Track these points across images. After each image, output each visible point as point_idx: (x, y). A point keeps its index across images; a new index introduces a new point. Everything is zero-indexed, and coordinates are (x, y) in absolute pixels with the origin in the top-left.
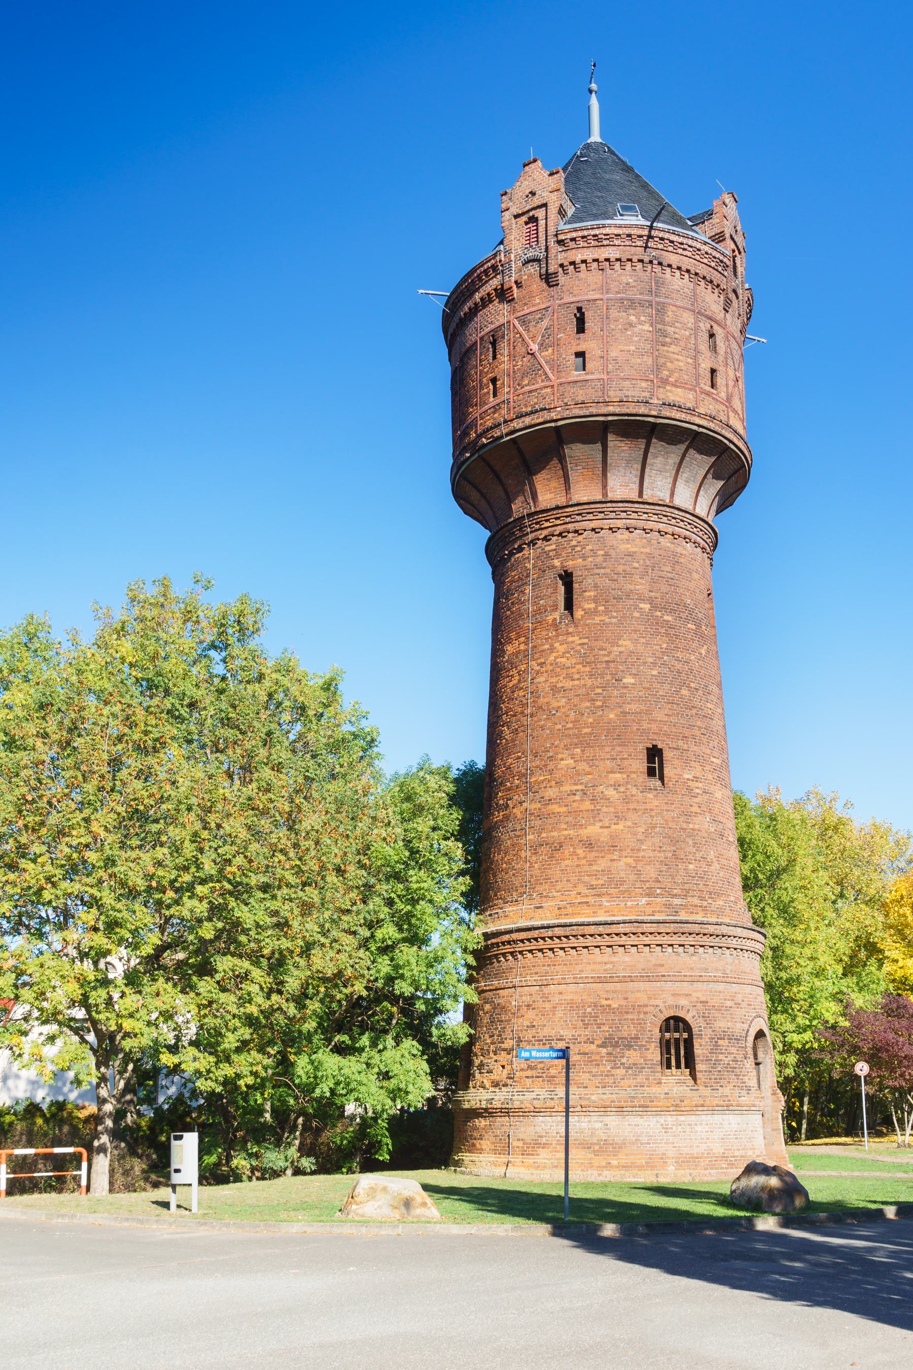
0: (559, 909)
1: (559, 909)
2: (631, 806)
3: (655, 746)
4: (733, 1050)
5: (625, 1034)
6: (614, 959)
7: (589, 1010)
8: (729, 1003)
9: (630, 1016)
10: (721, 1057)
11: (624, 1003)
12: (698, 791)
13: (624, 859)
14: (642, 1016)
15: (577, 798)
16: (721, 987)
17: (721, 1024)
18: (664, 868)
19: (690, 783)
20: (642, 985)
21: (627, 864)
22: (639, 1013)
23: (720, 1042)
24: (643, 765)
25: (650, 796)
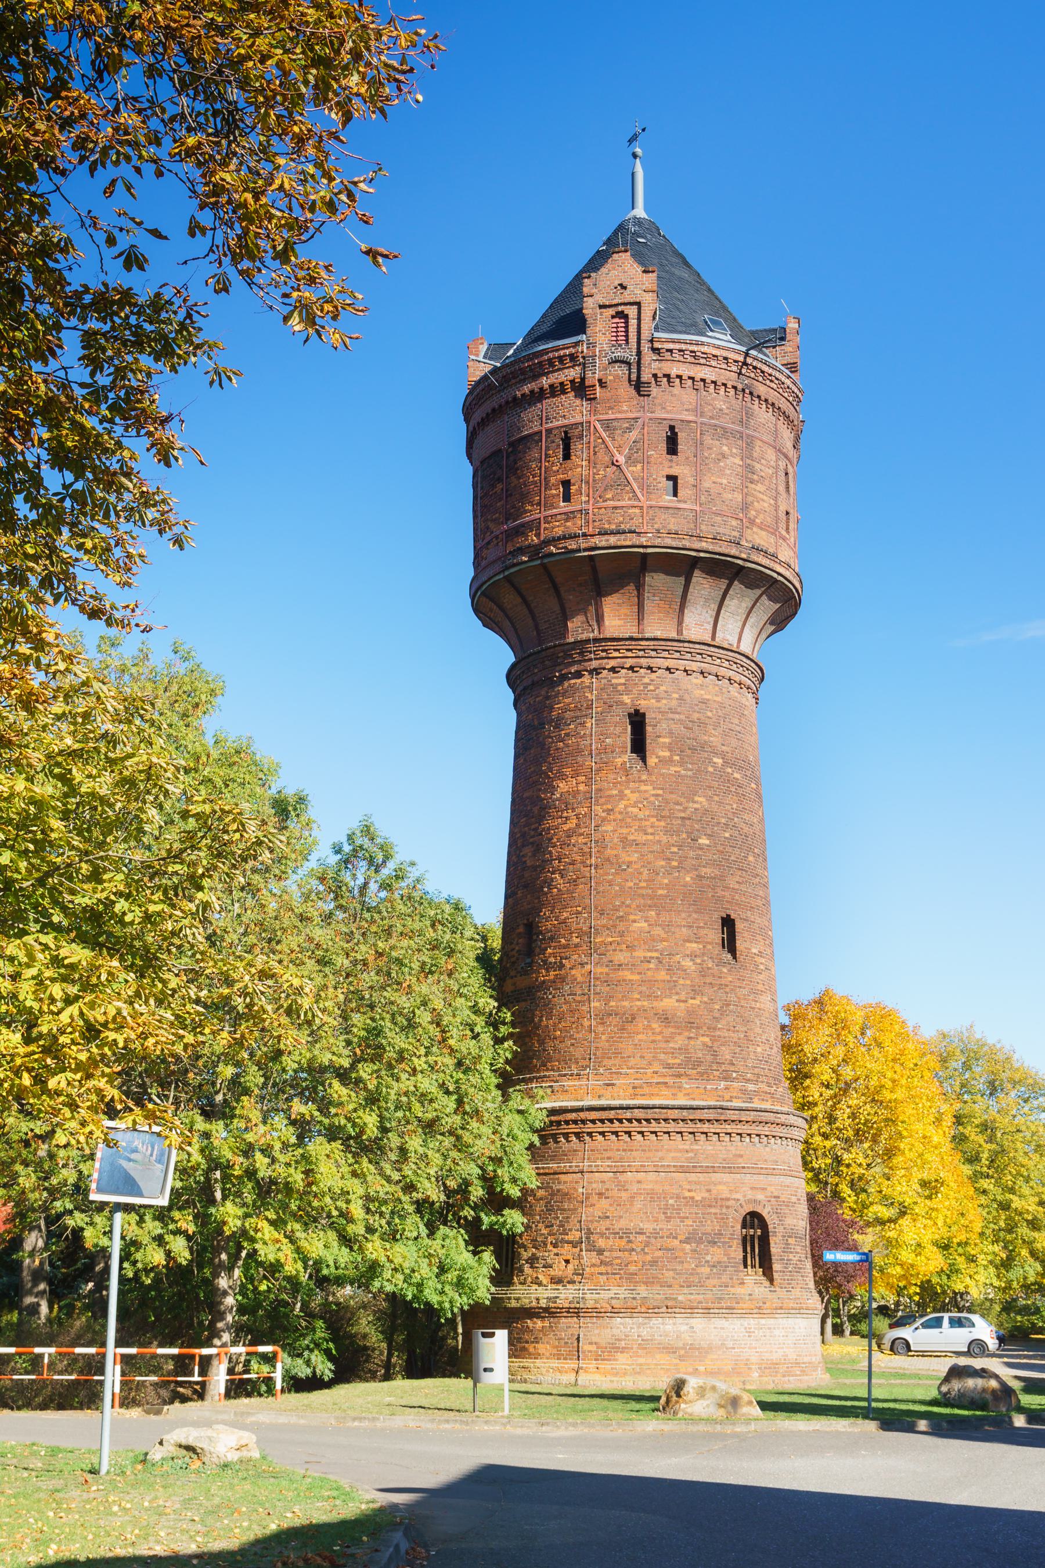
2: (708, 980)
3: (728, 916)
5: (709, 1229)
7: (671, 1202)
9: (713, 1210)
11: (706, 1195)
13: (701, 1039)
14: (724, 1210)
15: (652, 966)
20: (726, 1177)
21: (704, 1044)
25: (725, 970)
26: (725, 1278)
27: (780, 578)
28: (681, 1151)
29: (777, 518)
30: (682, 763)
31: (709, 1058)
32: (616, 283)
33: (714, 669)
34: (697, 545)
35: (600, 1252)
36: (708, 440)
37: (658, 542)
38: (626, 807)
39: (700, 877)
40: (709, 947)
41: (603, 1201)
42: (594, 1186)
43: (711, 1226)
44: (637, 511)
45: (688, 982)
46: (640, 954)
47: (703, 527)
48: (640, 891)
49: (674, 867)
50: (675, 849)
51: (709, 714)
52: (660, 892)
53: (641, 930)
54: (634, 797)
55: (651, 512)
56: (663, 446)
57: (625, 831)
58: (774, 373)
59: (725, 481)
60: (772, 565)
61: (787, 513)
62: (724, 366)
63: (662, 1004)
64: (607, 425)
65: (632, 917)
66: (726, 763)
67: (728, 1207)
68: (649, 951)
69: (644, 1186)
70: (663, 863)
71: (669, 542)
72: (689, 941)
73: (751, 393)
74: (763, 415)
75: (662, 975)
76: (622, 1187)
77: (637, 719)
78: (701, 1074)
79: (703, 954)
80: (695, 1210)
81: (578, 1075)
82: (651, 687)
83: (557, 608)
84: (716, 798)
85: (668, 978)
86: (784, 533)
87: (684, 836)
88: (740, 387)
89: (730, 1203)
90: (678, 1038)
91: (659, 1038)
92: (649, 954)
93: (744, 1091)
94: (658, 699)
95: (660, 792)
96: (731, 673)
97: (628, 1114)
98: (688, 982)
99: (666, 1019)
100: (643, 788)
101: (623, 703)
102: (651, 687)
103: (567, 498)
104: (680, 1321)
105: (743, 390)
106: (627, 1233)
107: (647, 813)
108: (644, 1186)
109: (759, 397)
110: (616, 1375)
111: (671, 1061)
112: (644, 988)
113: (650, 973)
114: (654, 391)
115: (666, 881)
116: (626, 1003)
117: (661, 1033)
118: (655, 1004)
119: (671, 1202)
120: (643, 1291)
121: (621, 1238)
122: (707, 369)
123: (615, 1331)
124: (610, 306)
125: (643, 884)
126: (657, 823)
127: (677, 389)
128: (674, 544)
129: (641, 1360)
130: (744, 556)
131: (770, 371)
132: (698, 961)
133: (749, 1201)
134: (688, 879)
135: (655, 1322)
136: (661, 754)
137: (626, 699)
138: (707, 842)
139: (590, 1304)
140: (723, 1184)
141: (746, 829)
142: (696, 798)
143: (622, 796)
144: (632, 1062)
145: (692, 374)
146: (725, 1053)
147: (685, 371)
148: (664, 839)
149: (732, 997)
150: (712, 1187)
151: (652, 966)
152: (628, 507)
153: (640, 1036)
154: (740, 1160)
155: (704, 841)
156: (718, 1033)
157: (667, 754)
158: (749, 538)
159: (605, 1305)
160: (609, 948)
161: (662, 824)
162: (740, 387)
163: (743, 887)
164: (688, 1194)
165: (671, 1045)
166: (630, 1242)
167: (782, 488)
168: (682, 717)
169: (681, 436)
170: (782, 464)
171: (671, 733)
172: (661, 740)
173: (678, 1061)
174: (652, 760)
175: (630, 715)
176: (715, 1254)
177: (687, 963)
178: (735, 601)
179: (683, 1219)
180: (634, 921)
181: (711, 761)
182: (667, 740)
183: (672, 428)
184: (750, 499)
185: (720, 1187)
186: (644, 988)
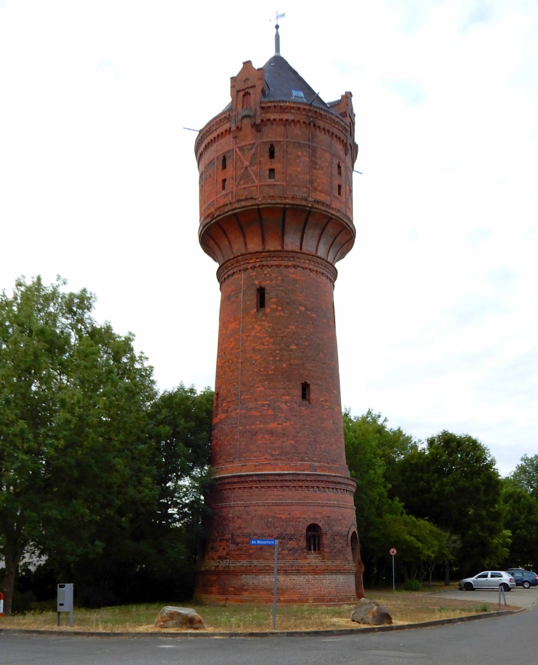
0: (255, 466)
1: (255, 466)
2: (294, 413)
3: (306, 383)
4: (342, 541)
5: (288, 532)
6: (284, 493)
7: (270, 520)
8: (340, 518)
9: (291, 523)
10: (336, 545)
11: (288, 516)
12: (327, 407)
13: (289, 441)
14: (297, 523)
15: (265, 408)
16: (336, 509)
17: (336, 528)
18: (309, 447)
19: (323, 403)
20: (298, 508)
21: (291, 444)
22: (296, 521)
23: (336, 537)
24: (299, 392)
25: (303, 408)
26: (296, 556)
30: (282, 310)
34: (284, 201)
35: (237, 544)
37: (264, 202)
39: (291, 364)
40: (295, 397)
43: (290, 530)
45: (283, 415)
46: (260, 403)
49: (278, 360)
50: (278, 352)
52: (270, 372)
57: (255, 345)
63: (270, 426)
65: (257, 385)
67: (299, 522)
68: (265, 401)
70: (272, 359)
71: (269, 201)
72: (284, 395)
75: (270, 412)
76: (248, 513)
78: (289, 459)
79: (292, 401)
84: (301, 326)
85: (273, 413)
87: (283, 345)
89: (299, 520)
91: (268, 442)
92: (265, 403)
95: (271, 325)
97: (250, 479)
98: (283, 415)
99: (271, 433)
106: (249, 535)
107: (265, 335)
110: (242, 602)
111: (274, 453)
113: (264, 411)
115: (273, 367)
116: (253, 427)
117: (269, 440)
118: (267, 426)
120: (255, 562)
121: (246, 537)
123: (243, 582)
126: (269, 340)
128: (272, 202)
129: (254, 595)
132: (289, 404)
133: (312, 519)
134: (284, 366)
135: (261, 577)
138: (295, 347)
139: (232, 569)
143: (253, 328)
148: (273, 347)
151: (265, 408)
153: (260, 442)
155: (293, 347)
157: (275, 306)
159: (238, 569)
161: (272, 340)
165: (274, 445)
171: (277, 296)
172: (273, 300)
173: (277, 453)
176: (292, 544)
177: (283, 406)
179: (275, 528)
182: (275, 300)
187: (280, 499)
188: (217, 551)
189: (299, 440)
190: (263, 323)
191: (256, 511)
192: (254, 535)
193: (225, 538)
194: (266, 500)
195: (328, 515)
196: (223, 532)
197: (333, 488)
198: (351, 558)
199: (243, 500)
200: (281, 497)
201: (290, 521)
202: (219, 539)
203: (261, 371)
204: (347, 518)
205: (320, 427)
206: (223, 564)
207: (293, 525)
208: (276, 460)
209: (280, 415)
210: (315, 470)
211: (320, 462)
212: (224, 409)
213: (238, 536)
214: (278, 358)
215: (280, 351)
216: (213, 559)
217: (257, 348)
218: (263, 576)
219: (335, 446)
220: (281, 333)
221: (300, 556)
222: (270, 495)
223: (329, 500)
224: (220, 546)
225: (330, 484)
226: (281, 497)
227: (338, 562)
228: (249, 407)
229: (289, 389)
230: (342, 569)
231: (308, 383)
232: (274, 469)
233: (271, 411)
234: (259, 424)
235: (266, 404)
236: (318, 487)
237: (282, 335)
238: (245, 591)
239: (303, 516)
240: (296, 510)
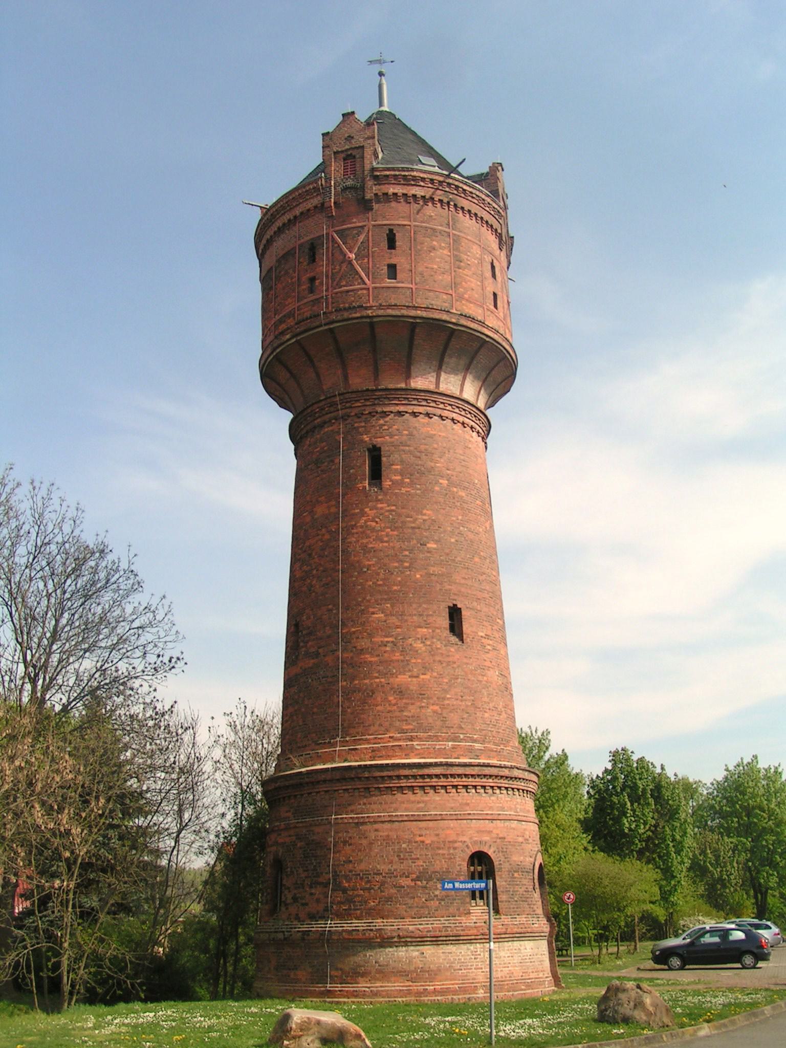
0: (373, 751)
1: (373, 751)
2: (437, 658)
3: (455, 605)
4: (525, 882)
5: (438, 868)
6: (426, 798)
7: (404, 846)
8: (520, 839)
9: (441, 852)
10: (517, 888)
11: (435, 839)
12: (489, 647)
13: (431, 707)
14: (452, 851)
15: (388, 649)
16: (514, 824)
17: (515, 858)
18: (466, 716)
19: (483, 640)
20: (452, 824)
21: (434, 712)
22: (449, 848)
23: (516, 875)
24: (445, 622)
25: (452, 650)
27: (487, 339)
28: (413, 802)
29: (484, 296)
31: (439, 723)
32: (346, 135)
33: (439, 412)
36: (420, 238)
38: (366, 521)
41: (347, 848)
42: (340, 835)
44: (365, 292)
45: (419, 661)
47: (419, 300)
48: (378, 588)
49: (406, 568)
50: (407, 553)
51: (435, 446)
53: (379, 620)
54: (372, 513)
55: (376, 291)
56: (385, 244)
58: (474, 191)
59: (435, 267)
60: (480, 328)
61: (495, 295)
62: (430, 185)
64: (341, 233)
66: (451, 484)
67: (455, 848)
69: (381, 834)
73: (455, 205)
74: (466, 222)
77: (375, 453)
80: (425, 852)
81: (329, 742)
82: (386, 427)
83: (313, 375)
85: (402, 658)
86: (492, 307)
88: (445, 200)
89: (456, 845)
90: (410, 707)
92: (386, 639)
93: (471, 750)
94: (391, 436)
95: (393, 508)
96: (466, 420)
98: (419, 661)
100: (380, 506)
101: (362, 441)
102: (386, 427)
103: (311, 291)
104: (412, 948)
105: (448, 203)
107: (383, 525)
108: (381, 834)
109: (462, 208)
112: (381, 668)
113: (386, 655)
114: (376, 206)
119: (404, 846)
122: (417, 188)
124: (342, 152)
125: (381, 583)
126: (391, 533)
127: (393, 204)
130: (454, 320)
131: (471, 190)
133: (475, 842)
134: (418, 576)
136: (394, 478)
137: (366, 438)
138: (435, 546)
140: (450, 829)
141: (471, 536)
142: (425, 511)
143: (363, 513)
144: (372, 729)
145: (405, 192)
146: (454, 718)
147: (399, 190)
149: (459, 672)
150: (440, 832)
151: (388, 649)
152: (358, 290)
153: (379, 708)
154: (468, 808)
156: (447, 702)
157: (399, 478)
158: (459, 308)
160: (354, 636)
161: (395, 533)
162: (445, 200)
163: (469, 583)
164: (418, 839)
165: (405, 714)
166: (369, 882)
167: (488, 274)
168: (412, 448)
169: (398, 236)
170: (488, 259)
171: (402, 462)
173: (412, 727)
174: (386, 483)
175: (369, 450)
177: (418, 645)
178: (454, 360)
180: (373, 613)
181: (437, 482)
183: (391, 231)
184: (458, 280)
185: (448, 832)
186: (381, 668)
187: (418, 810)
188: (306, 904)
189: (448, 704)
190: (380, 506)
191: (376, 830)
192: (374, 874)
193: (321, 880)
194: (396, 810)
195: (501, 835)
196: (315, 869)
197: (507, 788)
198: (540, 911)
199: (352, 811)
200: (422, 805)
201: (439, 848)
202: (308, 882)
203: (380, 585)
204: (531, 841)
205: (481, 681)
206: (317, 926)
207: (444, 854)
208: (411, 739)
209: (413, 661)
210: (477, 757)
211: (483, 742)
212: (312, 650)
213: (346, 876)
214: (407, 564)
215: (411, 551)
216: (297, 918)
217: (371, 546)
218: (395, 948)
219: (504, 715)
220: (410, 522)
221: (458, 909)
222: (403, 803)
223: (503, 809)
224: (312, 894)
225: (502, 781)
226: (422, 805)
227: (522, 919)
228: (359, 647)
229: (427, 616)
230: (529, 930)
231: (459, 606)
232: (407, 756)
233: (397, 654)
234: (377, 678)
235: (388, 642)
236: (484, 787)
237: (413, 525)
238: (362, 977)
239: (461, 838)
240: (448, 828)
